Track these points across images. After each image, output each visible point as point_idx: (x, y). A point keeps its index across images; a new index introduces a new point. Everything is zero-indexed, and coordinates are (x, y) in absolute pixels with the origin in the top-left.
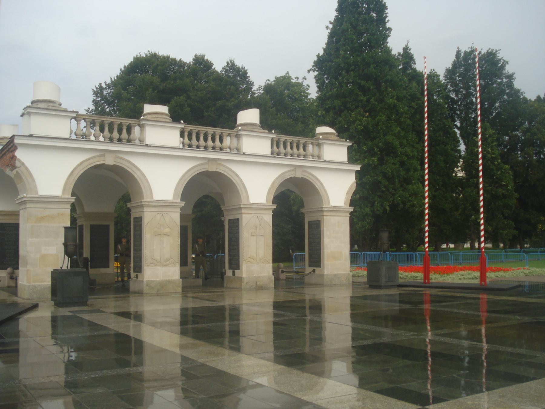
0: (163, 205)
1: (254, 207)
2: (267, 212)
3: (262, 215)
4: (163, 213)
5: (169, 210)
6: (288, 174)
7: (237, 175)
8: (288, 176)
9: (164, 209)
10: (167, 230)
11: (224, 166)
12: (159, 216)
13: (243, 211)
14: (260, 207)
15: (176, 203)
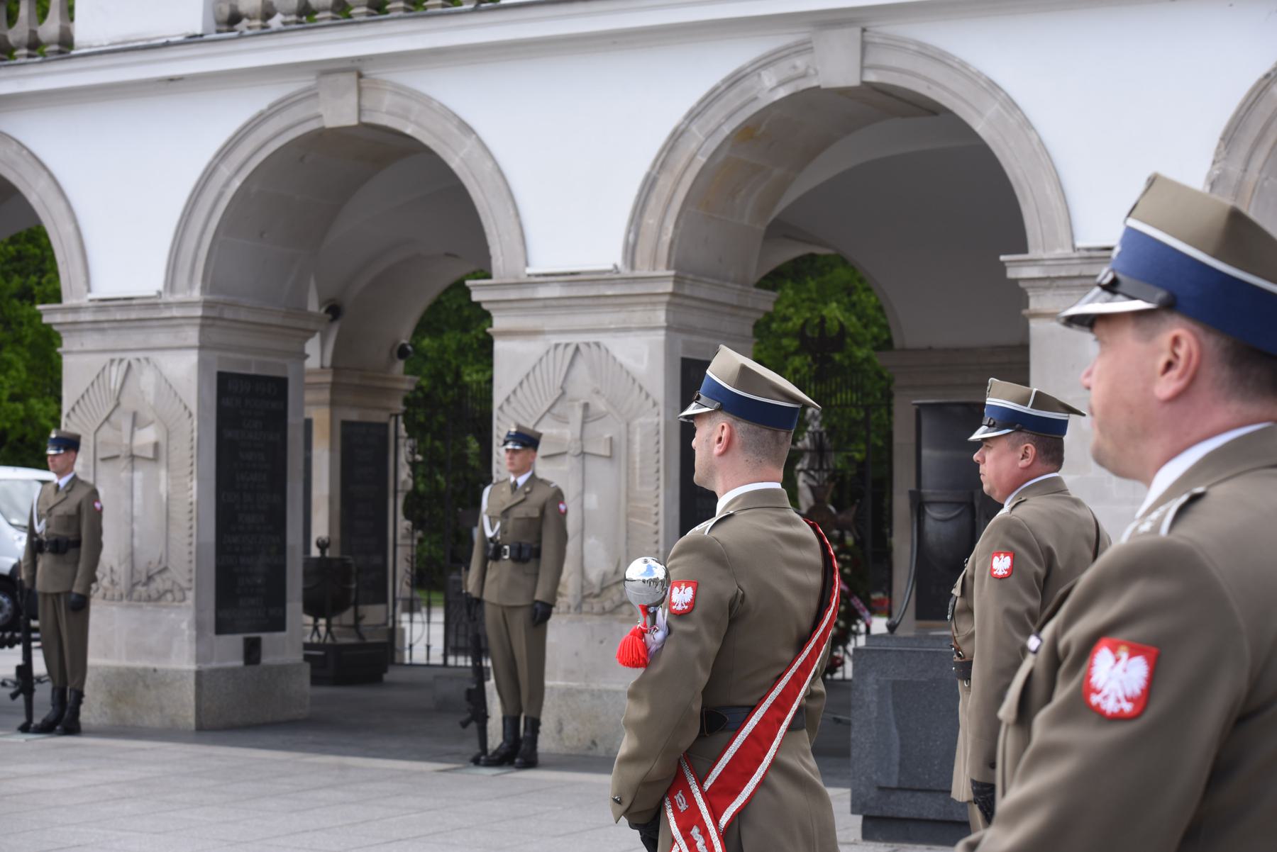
0: (128, 315)
1: (543, 292)
2: (638, 316)
3: (605, 339)
4: (130, 356)
5: (161, 338)
6: (768, 79)
7: (467, 129)
8: (771, 88)
9: (135, 338)
10: (147, 437)
11: (399, 90)
12: (116, 374)
13: (500, 322)
14: (583, 290)
15: (168, 305)
